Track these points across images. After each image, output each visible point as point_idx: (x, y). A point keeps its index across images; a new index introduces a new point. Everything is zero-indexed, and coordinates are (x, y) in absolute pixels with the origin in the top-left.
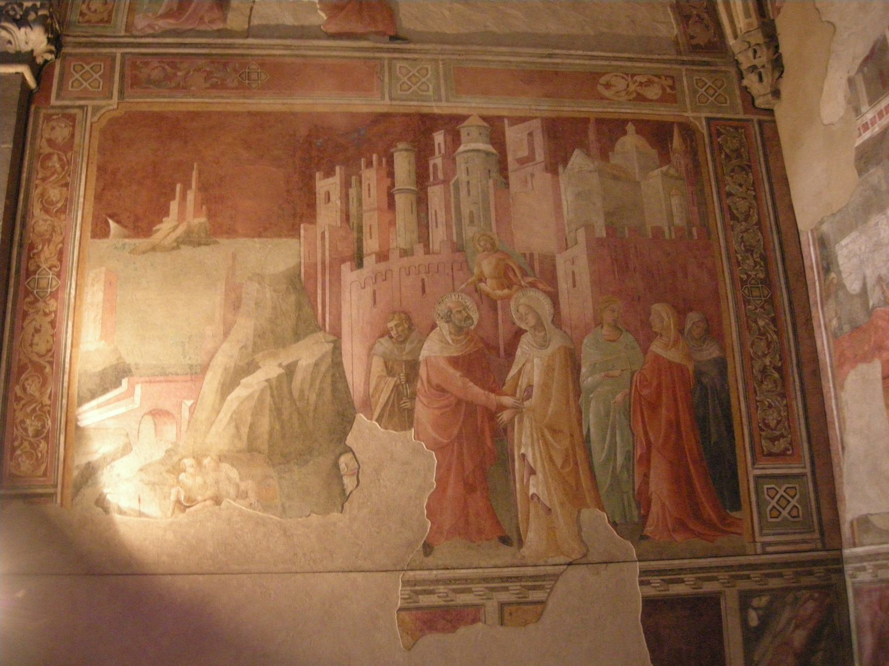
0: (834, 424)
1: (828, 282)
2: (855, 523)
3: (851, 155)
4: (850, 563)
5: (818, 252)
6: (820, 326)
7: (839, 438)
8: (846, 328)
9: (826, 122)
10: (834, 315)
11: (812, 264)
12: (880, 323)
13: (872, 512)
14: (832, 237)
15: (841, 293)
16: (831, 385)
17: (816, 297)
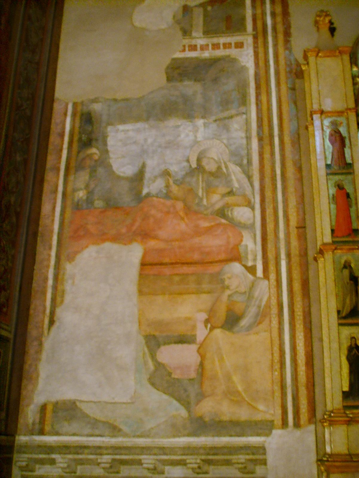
0: (44, 293)
1: (82, 155)
2: (50, 408)
3: (168, 61)
4: (24, 453)
5: (77, 124)
6: (55, 191)
7: (48, 311)
8: (99, 204)
9: (137, 24)
10: (83, 187)
11: (63, 132)
12: (153, 212)
13: (84, 398)
14: (105, 118)
15: (101, 171)
16: (53, 253)
17: (60, 163)
